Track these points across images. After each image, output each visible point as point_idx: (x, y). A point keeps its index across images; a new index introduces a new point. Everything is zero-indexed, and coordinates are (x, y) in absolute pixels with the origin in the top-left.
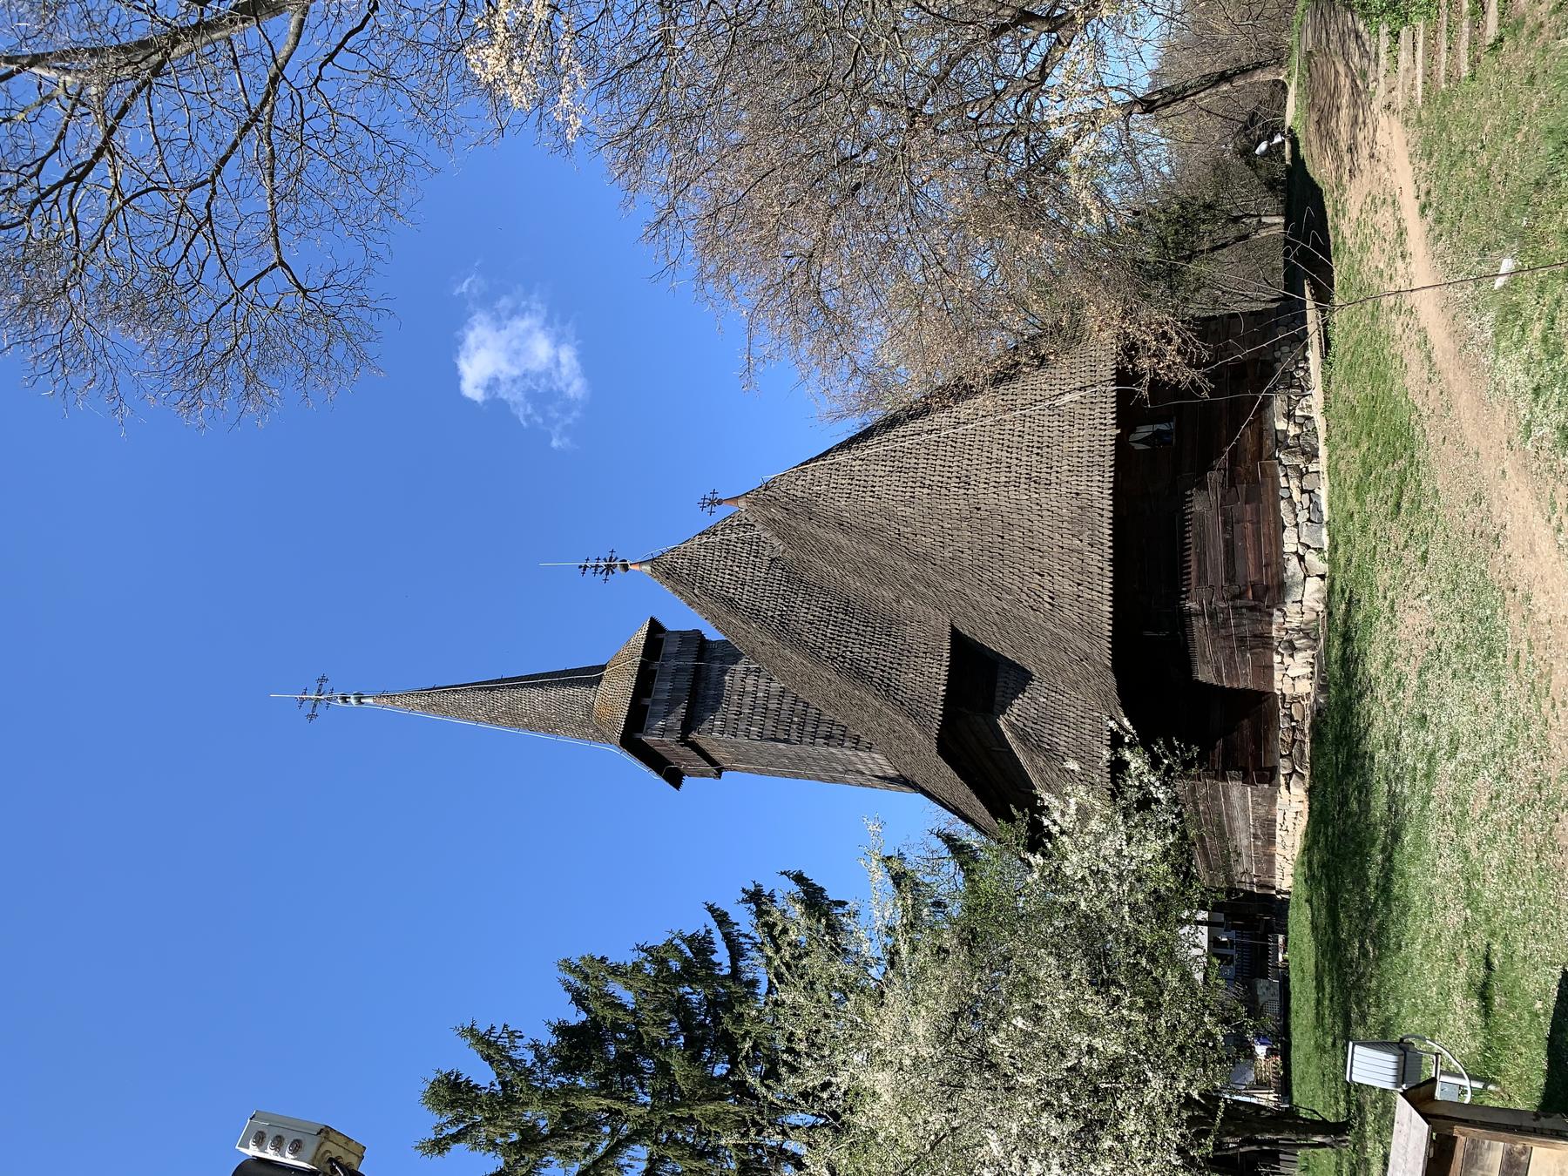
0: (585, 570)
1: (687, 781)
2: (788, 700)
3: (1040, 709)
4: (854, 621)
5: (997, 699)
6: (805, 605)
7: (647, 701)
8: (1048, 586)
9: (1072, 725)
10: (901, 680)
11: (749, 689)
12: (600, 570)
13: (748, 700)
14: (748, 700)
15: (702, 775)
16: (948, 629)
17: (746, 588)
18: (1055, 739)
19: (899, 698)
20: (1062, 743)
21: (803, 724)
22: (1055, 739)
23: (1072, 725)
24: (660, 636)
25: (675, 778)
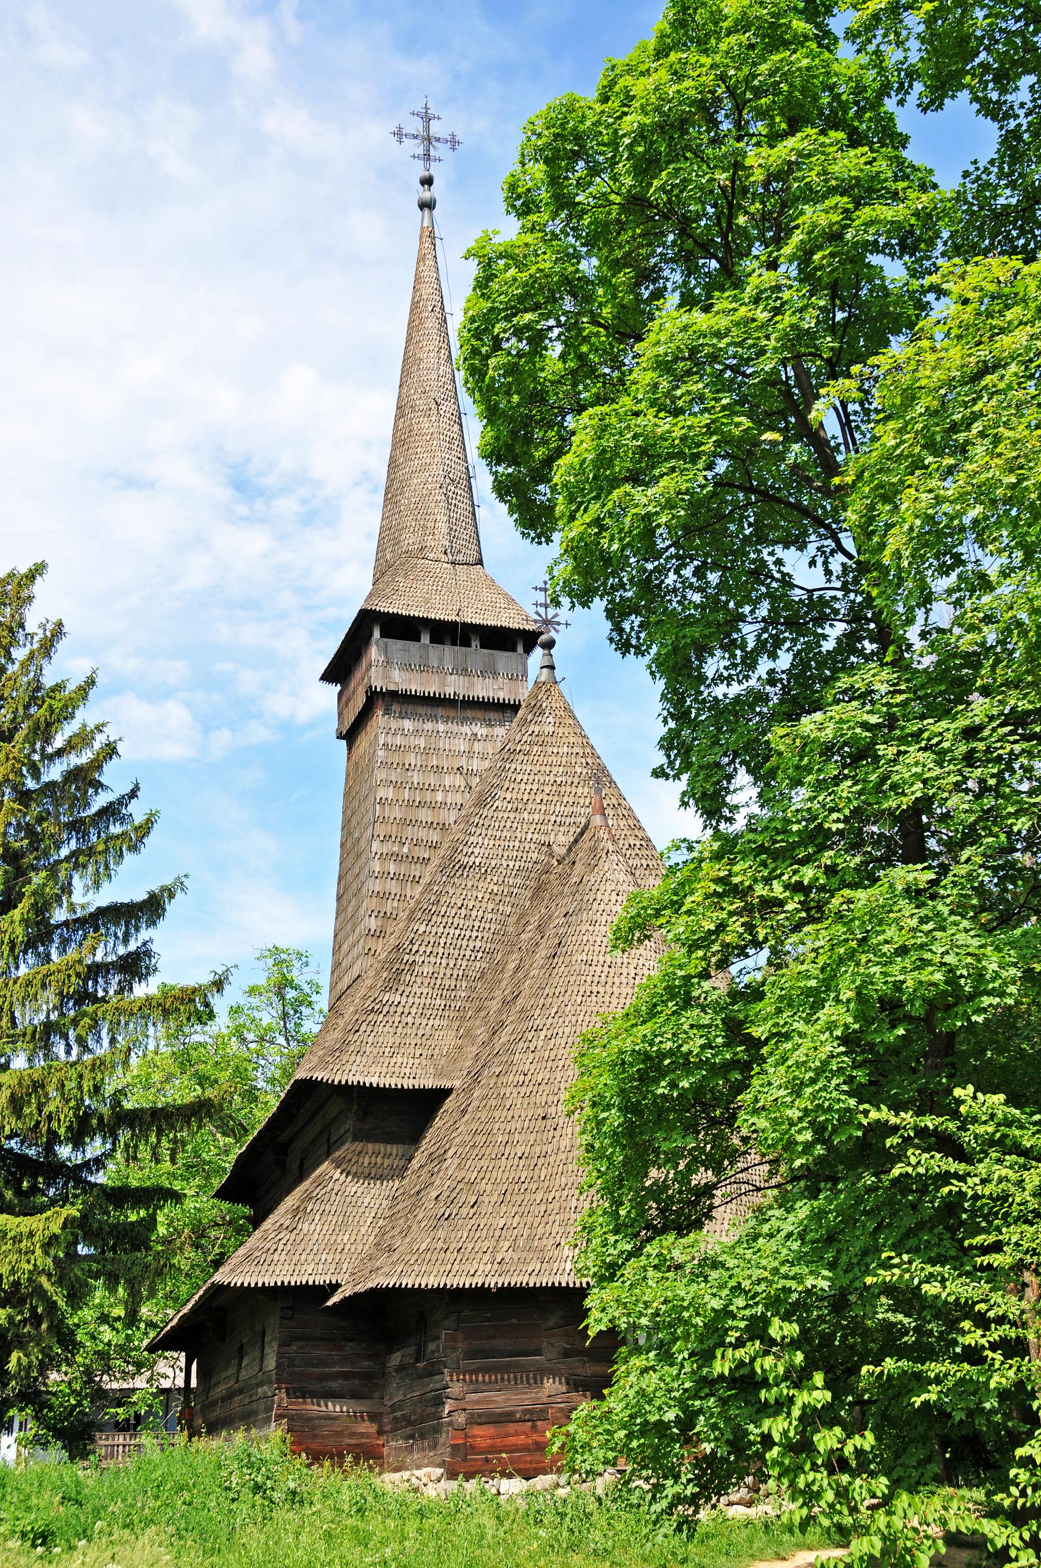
0: (541, 589)
1: (333, 690)
2: (435, 836)
3: (354, 1199)
4: (465, 963)
5: (370, 1146)
6: (487, 896)
7: (425, 639)
8: (464, 1211)
9: (333, 1238)
10: (386, 1029)
11: (448, 780)
12: (542, 611)
13: (432, 779)
14: (432, 779)
15: (340, 714)
16: (449, 1085)
17: (512, 815)
18: (317, 1217)
19: (363, 1028)
20: (313, 1227)
21: (398, 858)
22: (317, 1217)
23: (333, 1238)
24: (520, 649)
25: (330, 676)
